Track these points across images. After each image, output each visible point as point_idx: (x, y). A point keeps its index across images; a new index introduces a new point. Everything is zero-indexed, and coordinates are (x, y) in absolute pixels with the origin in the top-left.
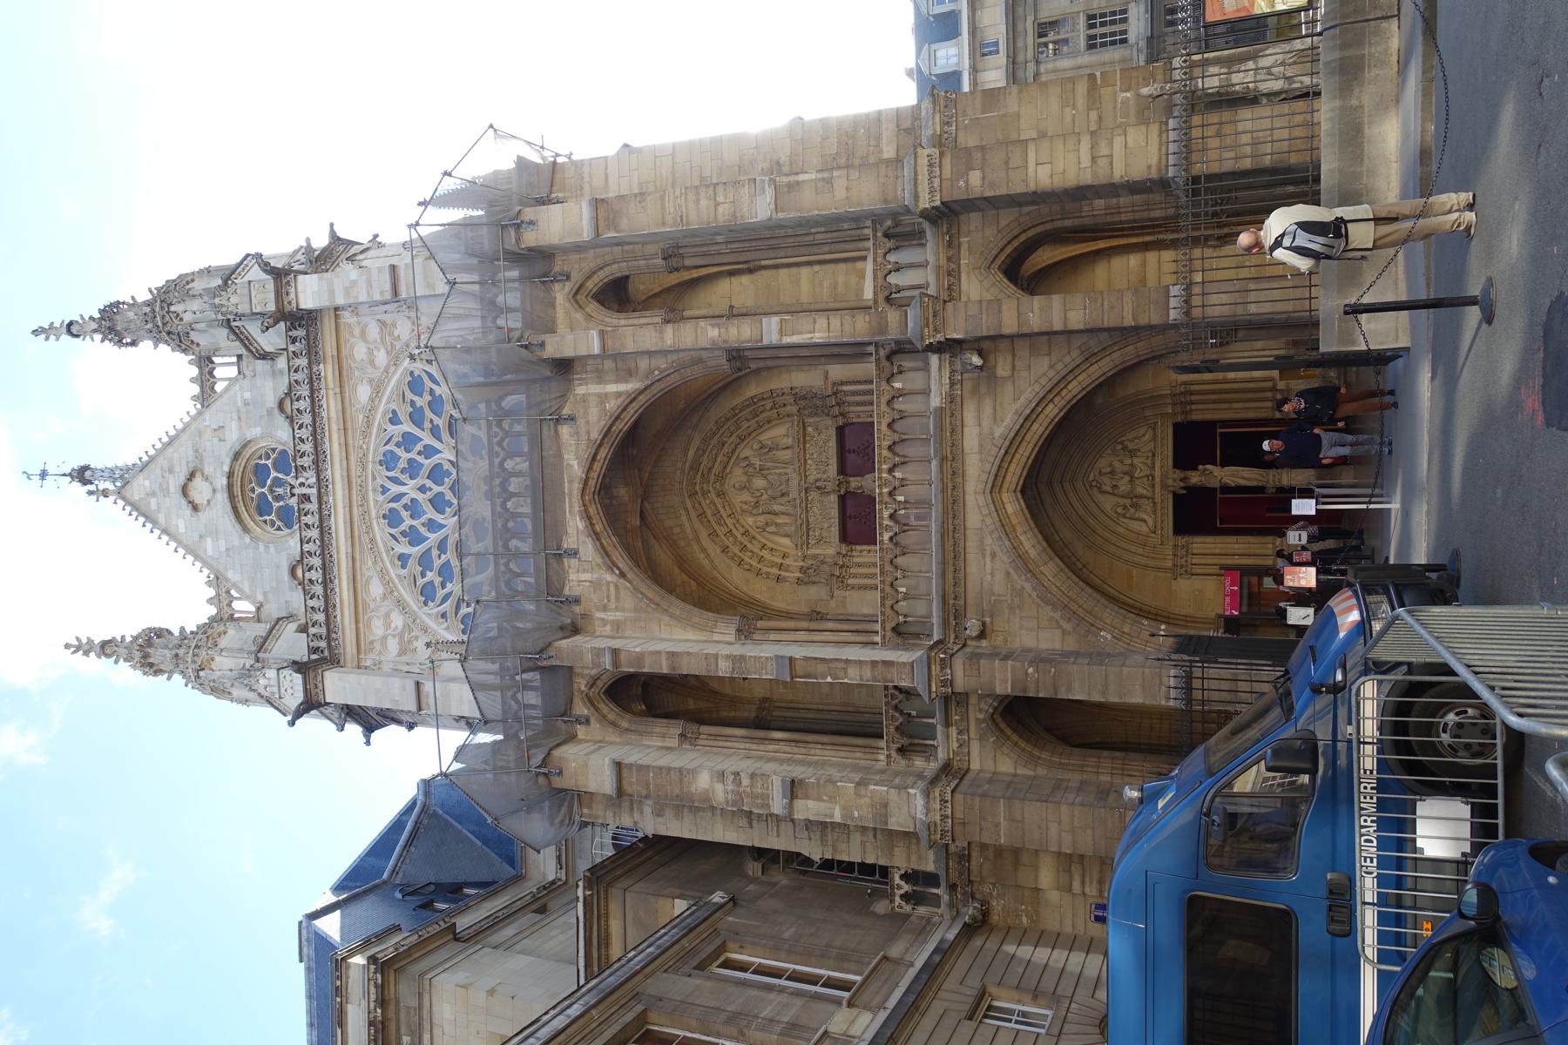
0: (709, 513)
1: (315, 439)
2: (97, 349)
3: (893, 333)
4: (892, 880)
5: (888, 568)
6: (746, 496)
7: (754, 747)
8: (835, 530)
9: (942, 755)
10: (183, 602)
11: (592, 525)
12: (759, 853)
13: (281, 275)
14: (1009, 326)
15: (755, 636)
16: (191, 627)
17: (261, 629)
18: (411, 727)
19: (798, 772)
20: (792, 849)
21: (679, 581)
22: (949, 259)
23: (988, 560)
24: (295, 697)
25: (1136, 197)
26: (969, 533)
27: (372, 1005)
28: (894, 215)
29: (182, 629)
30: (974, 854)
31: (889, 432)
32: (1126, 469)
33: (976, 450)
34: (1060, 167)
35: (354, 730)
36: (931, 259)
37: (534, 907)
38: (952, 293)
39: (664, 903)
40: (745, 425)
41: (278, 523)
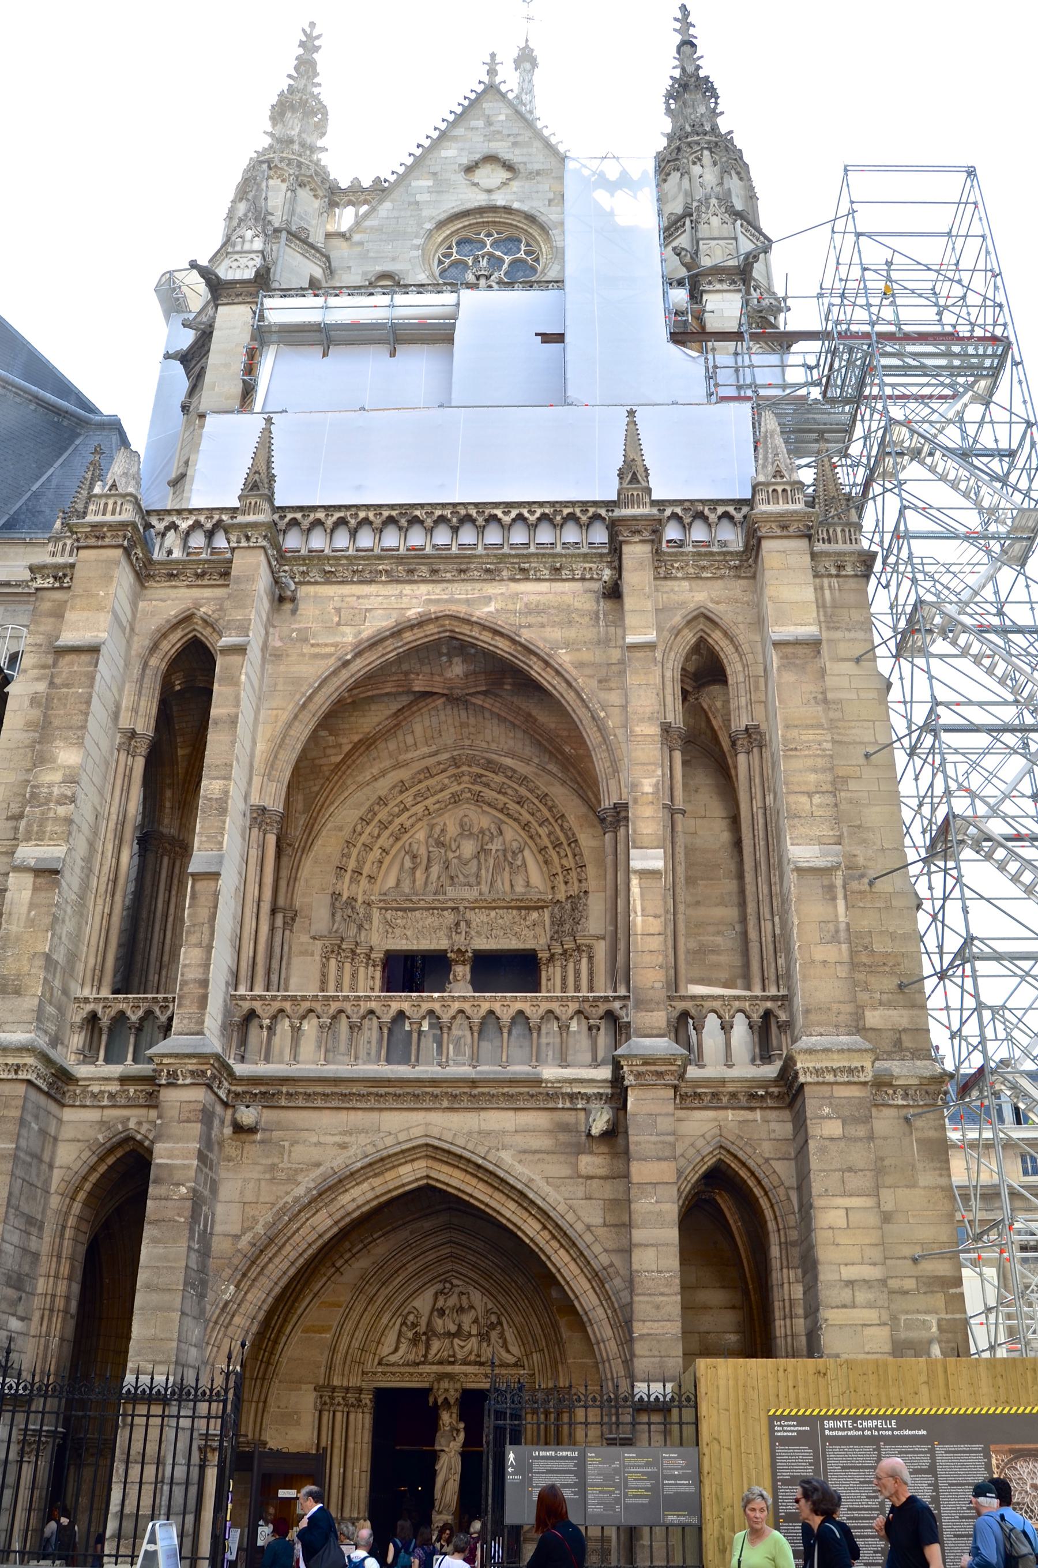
0: (431, 782)
2: (665, 70)
5: (334, 1006)
6: (453, 830)
11: (412, 627)
13: (741, 275)
15: (255, 831)
17: (317, 238)
19: (71, 880)
21: (344, 741)
22: (734, 1095)
23: (338, 1139)
25: (804, 1339)
26: (375, 1115)
29: (324, 149)
31: (512, 1011)
32: (466, 1327)
33: (484, 1126)
38: (689, 1097)
40: (543, 831)
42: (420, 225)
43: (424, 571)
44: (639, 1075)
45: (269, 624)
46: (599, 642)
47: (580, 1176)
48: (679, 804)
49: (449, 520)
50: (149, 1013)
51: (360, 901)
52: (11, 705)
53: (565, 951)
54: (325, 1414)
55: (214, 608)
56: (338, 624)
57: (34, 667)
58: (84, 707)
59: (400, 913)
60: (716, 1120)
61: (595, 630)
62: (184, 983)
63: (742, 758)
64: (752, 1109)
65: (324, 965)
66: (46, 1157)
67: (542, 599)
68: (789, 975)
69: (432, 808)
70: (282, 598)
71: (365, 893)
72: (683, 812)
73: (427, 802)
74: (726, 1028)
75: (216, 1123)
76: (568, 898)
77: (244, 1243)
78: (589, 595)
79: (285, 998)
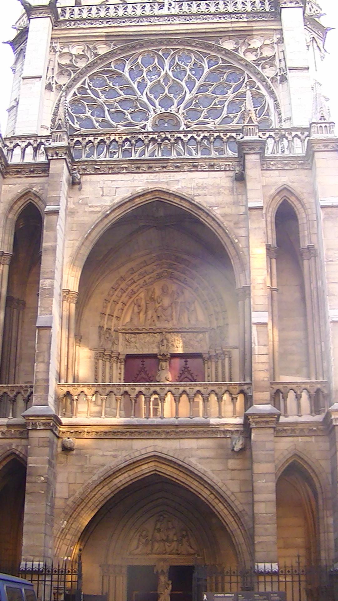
3: (257, 396)
5: (108, 389)
6: (158, 292)
8: (134, 351)
14: (258, 468)
18: (14, 70)
22: (302, 430)
26: (130, 442)
31: (195, 391)
32: (171, 537)
33: (182, 447)
38: (280, 431)
43: (145, 167)
44: (257, 423)
46: (234, 203)
47: (228, 469)
49: (157, 140)
50: (18, 393)
51: (113, 330)
54: (105, 578)
55: (40, 188)
56: (103, 196)
59: (133, 335)
60: (293, 442)
61: (231, 197)
63: (306, 262)
65: (96, 363)
68: (328, 371)
69: (148, 281)
70: (74, 183)
72: (277, 290)
73: (145, 278)
74: (298, 397)
75: (55, 446)
76: (218, 327)
77: (70, 502)
78: (228, 179)
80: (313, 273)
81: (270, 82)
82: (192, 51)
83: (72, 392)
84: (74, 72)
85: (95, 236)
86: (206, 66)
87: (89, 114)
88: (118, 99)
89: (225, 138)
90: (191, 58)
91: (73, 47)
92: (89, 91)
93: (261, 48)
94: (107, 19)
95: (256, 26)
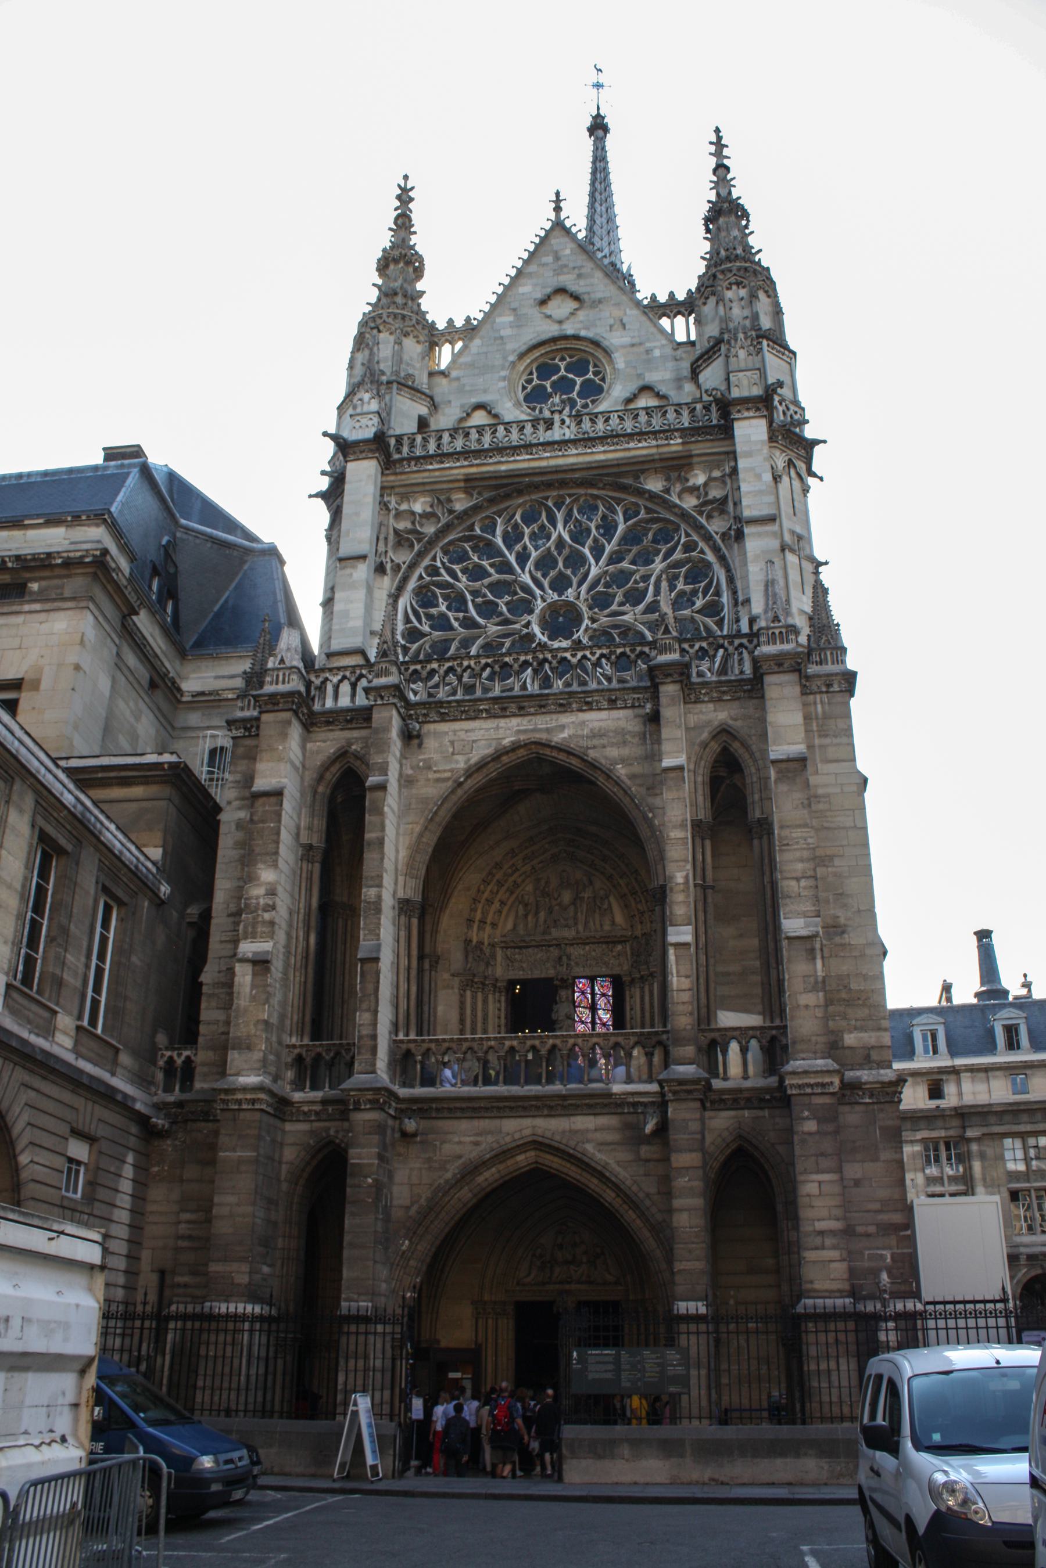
1: (606, 437)
2: (702, 196)
4: (186, 1049)
5: (465, 1045)
7: (301, 917)
9: (297, 1096)
10: (452, 295)
11: (507, 753)
12: (206, 916)
14: (683, 1159)
15: (403, 918)
16: (425, 304)
17: (422, 380)
19: (277, 966)
20: (211, 955)
22: (748, 1100)
23: (472, 1139)
24: (351, 435)
26: (497, 1122)
27: (65, 555)
28: (785, 1048)
30: (210, 1125)
33: (573, 1127)
34: (817, 1203)
35: (324, 483)
36: (748, 1084)
37: (156, 678)
39: (158, 836)
41: (530, 387)
42: (505, 358)
43: (513, 708)
44: (675, 1093)
45: (403, 756)
48: (710, 881)
50: (338, 1054)
52: (223, 829)
53: (642, 977)
54: (480, 1321)
56: (453, 754)
57: (237, 799)
58: (275, 837)
62: (360, 1037)
64: (761, 1109)
66: (277, 1157)
67: (603, 724)
70: (410, 737)
71: (489, 936)
72: (712, 887)
75: (389, 1132)
79: (431, 1041)
80: (766, 861)
81: (719, 541)
82: (597, 497)
83: (413, 1051)
84: (419, 541)
85: (445, 815)
86: (620, 518)
87: (443, 608)
88: (486, 581)
89: (633, 656)
90: (596, 508)
91: (415, 501)
92: (442, 571)
93: (706, 484)
94: (466, 454)
95: (697, 449)
